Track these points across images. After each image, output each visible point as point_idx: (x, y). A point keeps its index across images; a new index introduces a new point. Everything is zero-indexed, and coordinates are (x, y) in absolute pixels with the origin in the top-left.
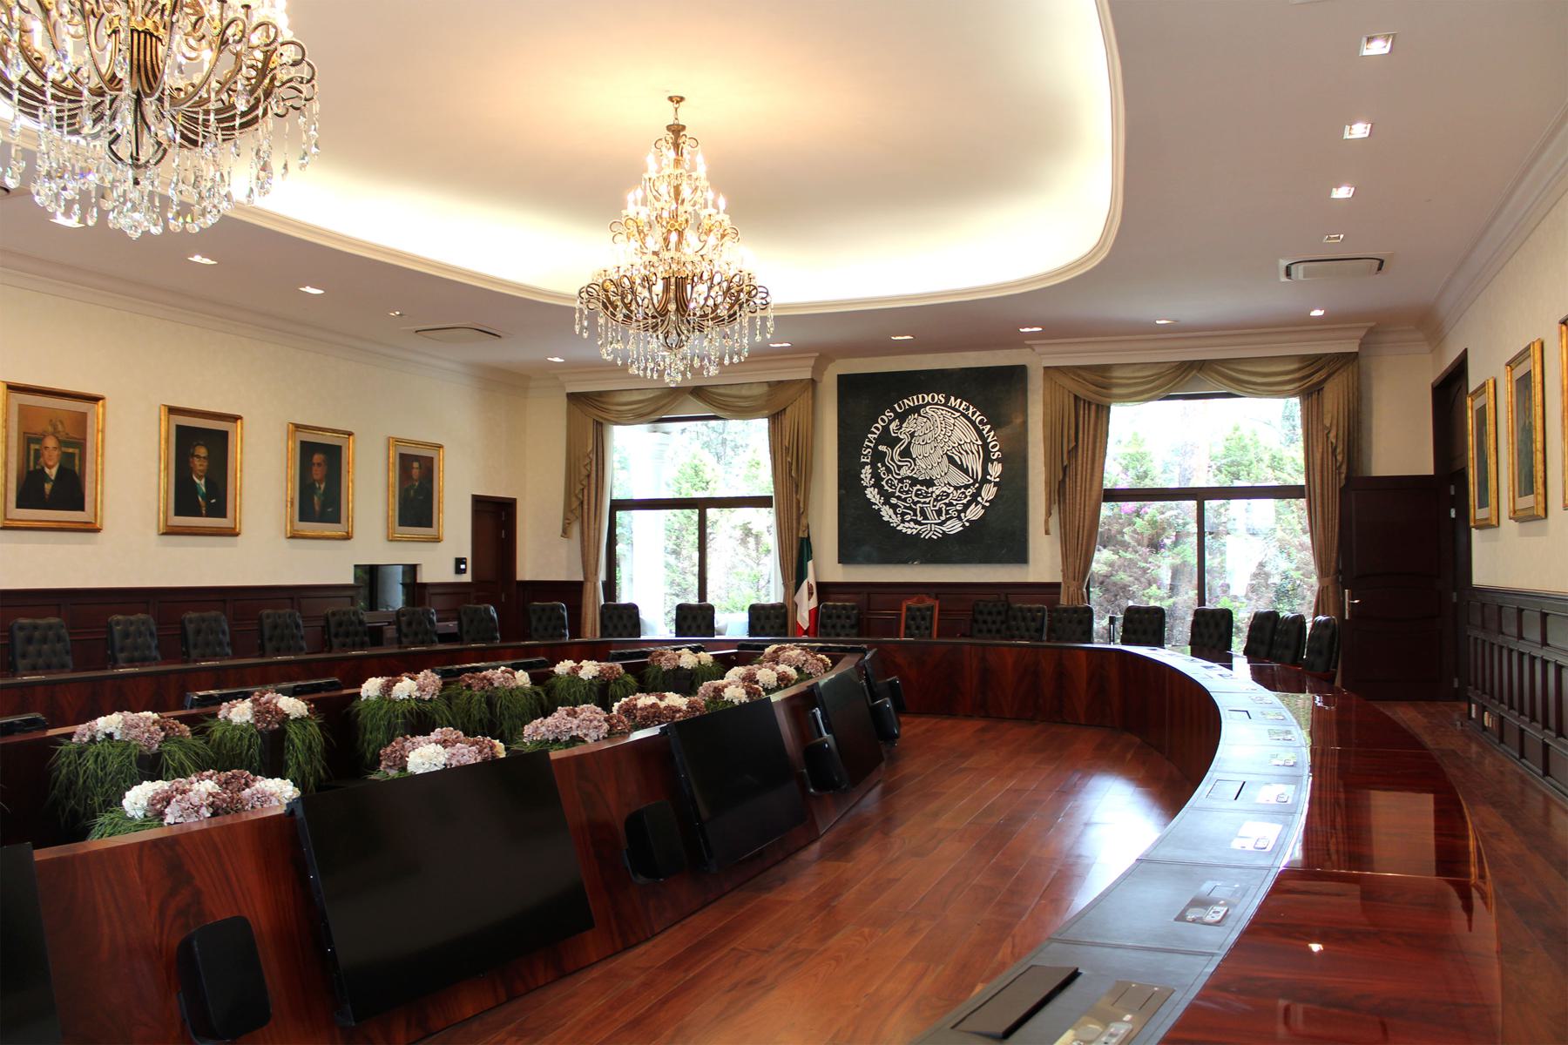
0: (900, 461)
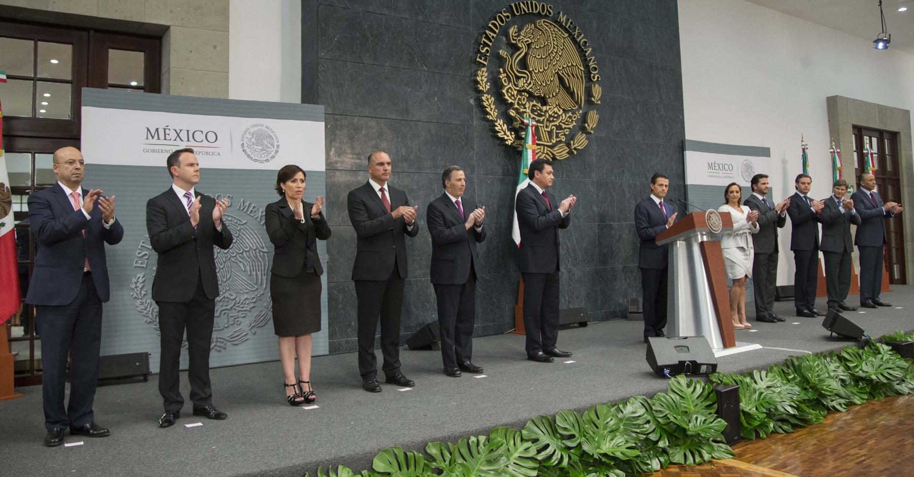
0: (518, 71)
